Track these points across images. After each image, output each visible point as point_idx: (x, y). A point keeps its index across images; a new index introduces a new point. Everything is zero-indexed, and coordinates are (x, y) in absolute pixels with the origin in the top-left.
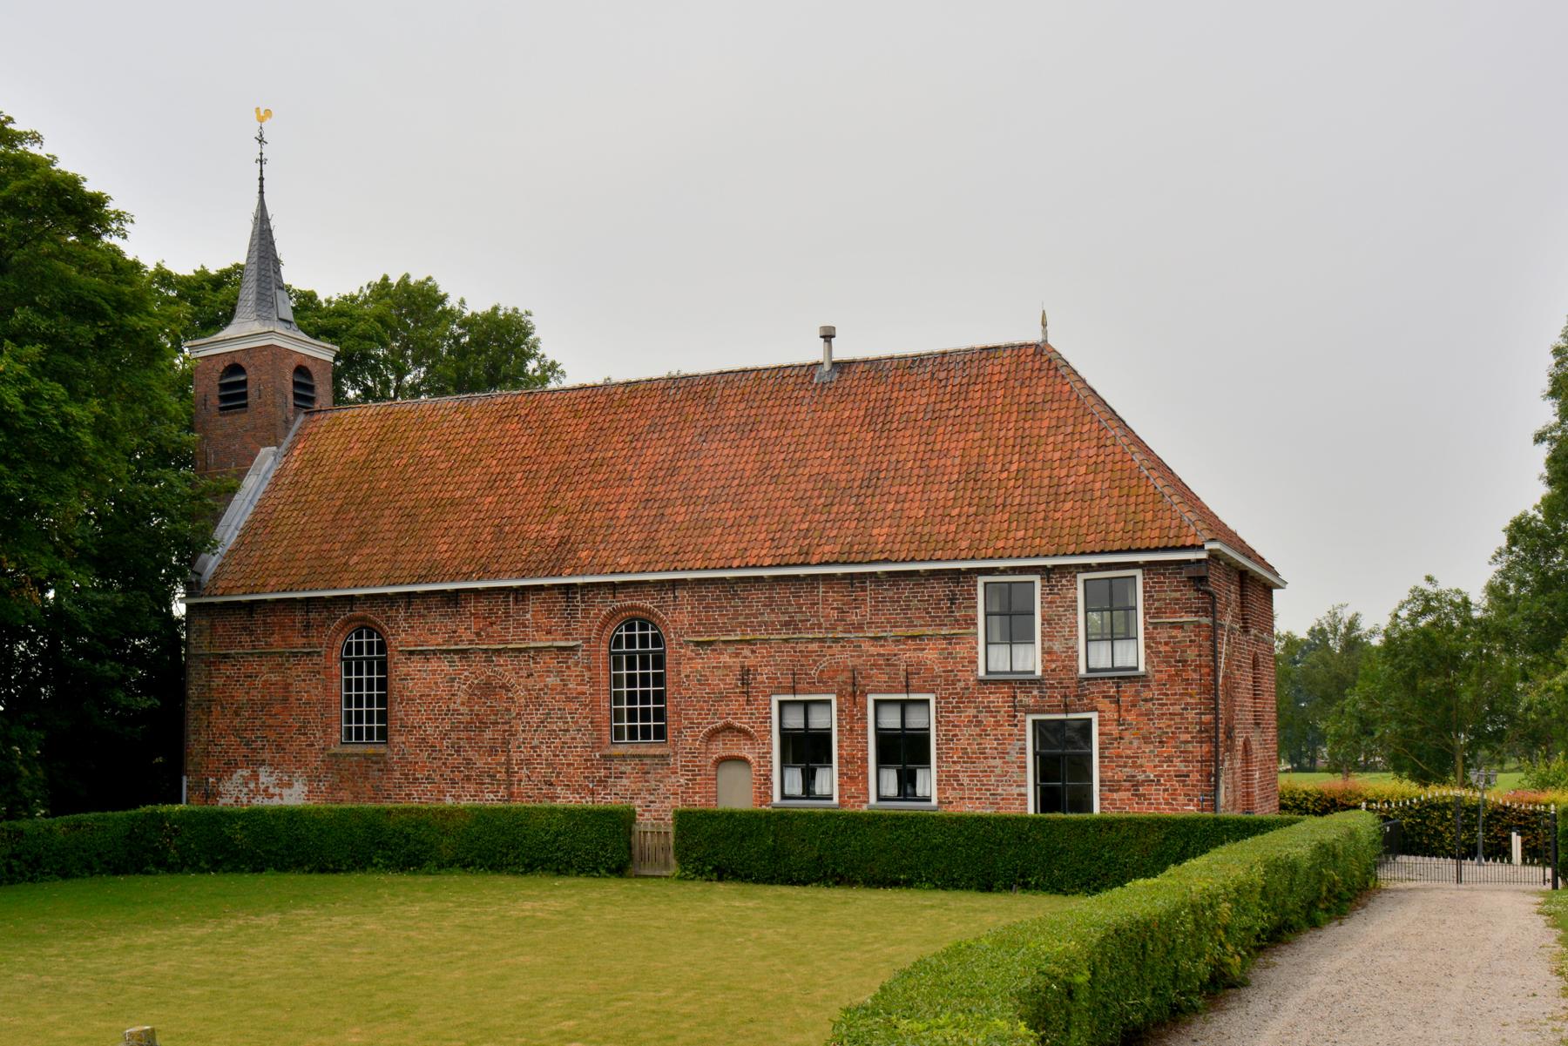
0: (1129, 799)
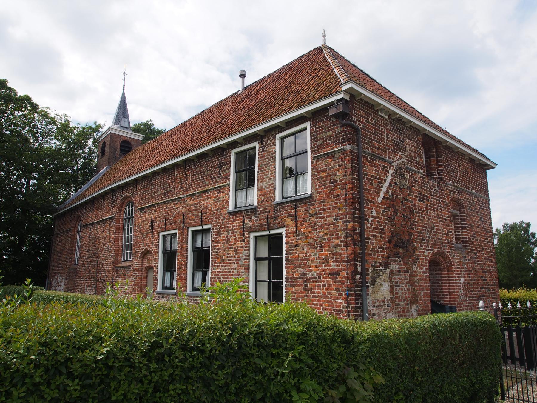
0: (302, 293)
